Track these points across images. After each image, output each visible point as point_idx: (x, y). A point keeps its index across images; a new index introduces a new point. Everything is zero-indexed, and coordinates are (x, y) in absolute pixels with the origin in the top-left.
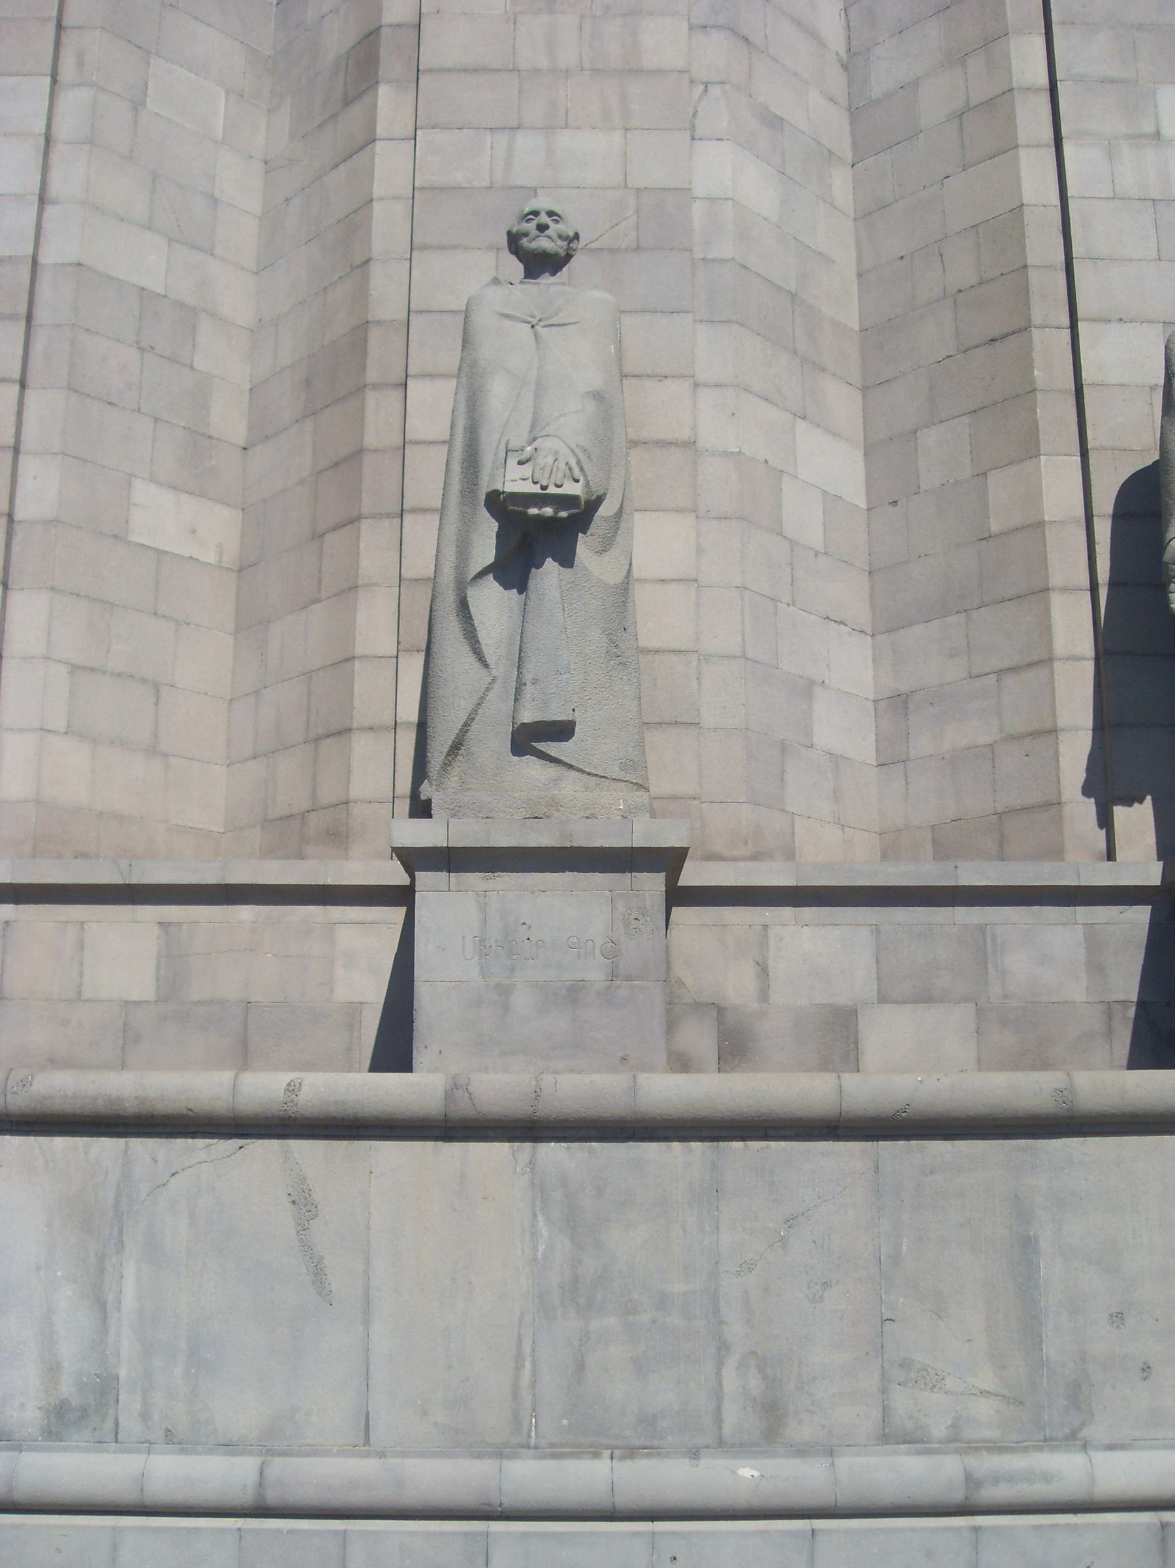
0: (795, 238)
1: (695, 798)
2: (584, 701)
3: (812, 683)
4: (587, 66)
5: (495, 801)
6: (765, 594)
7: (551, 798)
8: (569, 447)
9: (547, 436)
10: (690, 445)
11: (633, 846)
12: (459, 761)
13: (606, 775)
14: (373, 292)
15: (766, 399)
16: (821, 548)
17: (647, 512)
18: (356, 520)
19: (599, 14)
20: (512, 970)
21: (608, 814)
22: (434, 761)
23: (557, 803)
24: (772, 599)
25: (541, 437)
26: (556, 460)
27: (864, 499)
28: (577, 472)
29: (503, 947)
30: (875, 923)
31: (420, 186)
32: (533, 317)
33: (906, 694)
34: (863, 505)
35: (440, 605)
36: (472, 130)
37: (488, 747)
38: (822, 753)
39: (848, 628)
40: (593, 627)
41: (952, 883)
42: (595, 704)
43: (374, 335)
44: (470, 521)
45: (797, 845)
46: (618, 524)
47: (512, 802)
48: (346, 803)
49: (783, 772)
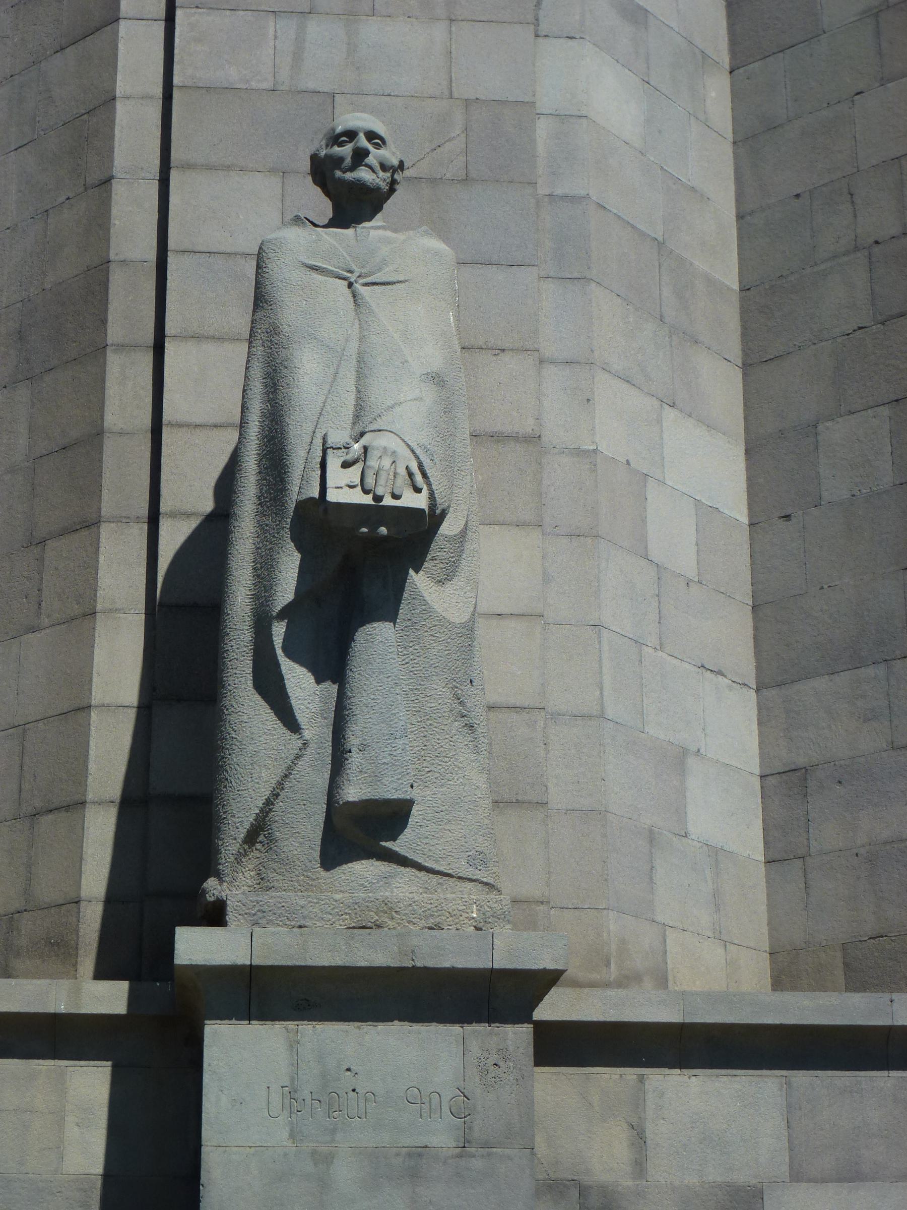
3: (684, 752)
5: (309, 905)
6: (627, 634)
7: (384, 901)
8: (408, 445)
9: (380, 431)
10: (532, 440)
11: (495, 967)
12: (256, 849)
13: (451, 871)
14: (117, 222)
15: (628, 381)
16: (692, 574)
20: (334, 1131)
22: (226, 850)
23: (391, 909)
24: (636, 642)
26: (394, 462)
27: (746, 512)
28: (419, 478)
29: (320, 1101)
31: (181, 85)
32: (351, 272)
33: (805, 768)
34: (744, 519)
36: (250, 13)
37: (298, 833)
39: (727, 681)
40: (434, 678)
41: (888, 1022)
43: (117, 279)
44: (274, 537)
45: (670, 966)
46: (462, 546)
48: (76, 902)
49: (652, 869)
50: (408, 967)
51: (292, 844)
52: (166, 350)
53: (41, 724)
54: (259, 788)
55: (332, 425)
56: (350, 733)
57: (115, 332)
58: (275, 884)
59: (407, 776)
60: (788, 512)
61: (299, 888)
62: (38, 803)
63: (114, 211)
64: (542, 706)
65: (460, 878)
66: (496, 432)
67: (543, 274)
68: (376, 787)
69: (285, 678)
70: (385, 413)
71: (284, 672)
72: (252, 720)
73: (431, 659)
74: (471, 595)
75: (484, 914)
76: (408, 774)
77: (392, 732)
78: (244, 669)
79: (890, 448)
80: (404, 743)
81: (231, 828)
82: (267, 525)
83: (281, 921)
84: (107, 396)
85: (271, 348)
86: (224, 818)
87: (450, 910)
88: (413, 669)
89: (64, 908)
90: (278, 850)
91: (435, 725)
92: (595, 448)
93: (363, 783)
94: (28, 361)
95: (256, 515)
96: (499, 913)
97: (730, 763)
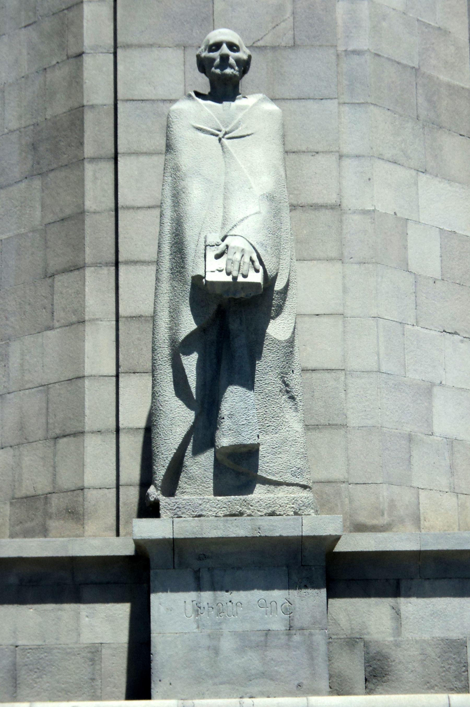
0: (418, 20)
1: (344, 482)
2: (265, 427)
7: (244, 500)
8: (251, 244)
9: (235, 235)
11: (303, 534)
14: (87, 81)
15: (395, 163)
16: (438, 275)
17: (305, 261)
18: (81, 268)
21: (284, 511)
23: (249, 504)
25: (231, 235)
35: (159, 355)
37: (197, 462)
38: (440, 439)
40: (270, 373)
42: (273, 429)
43: (89, 117)
47: (217, 504)
48: (82, 489)
49: (410, 457)
50: (257, 537)
51: (195, 469)
52: (118, 162)
53: (57, 385)
54: (176, 438)
55: (210, 229)
56: (224, 408)
58: (187, 490)
59: (256, 431)
61: (199, 492)
62: (58, 431)
64: (343, 368)
66: (314, 204)
67: (341, 101)
68: (239, 438)
69: (188, 376)
70: (238, 224)
71: (187, 373)
72: (171, 400)
73: (269, 363)
74: (291, 322)
75: (299, 505)
76: (256, 430)
77: (246, 407)
78: (165, 370)
80: (253, 413)
83: (189, 513)
84: (85, 190)
85: (176, 179)
86: (158, 455)
88: (258, 369)
89: (75, 492)
91: (272, 399)
92: (374, 208)
93: (231, 436)
94: (38, 163)
95: (170, 280)
96: (307, 504)
97: (462, 387)
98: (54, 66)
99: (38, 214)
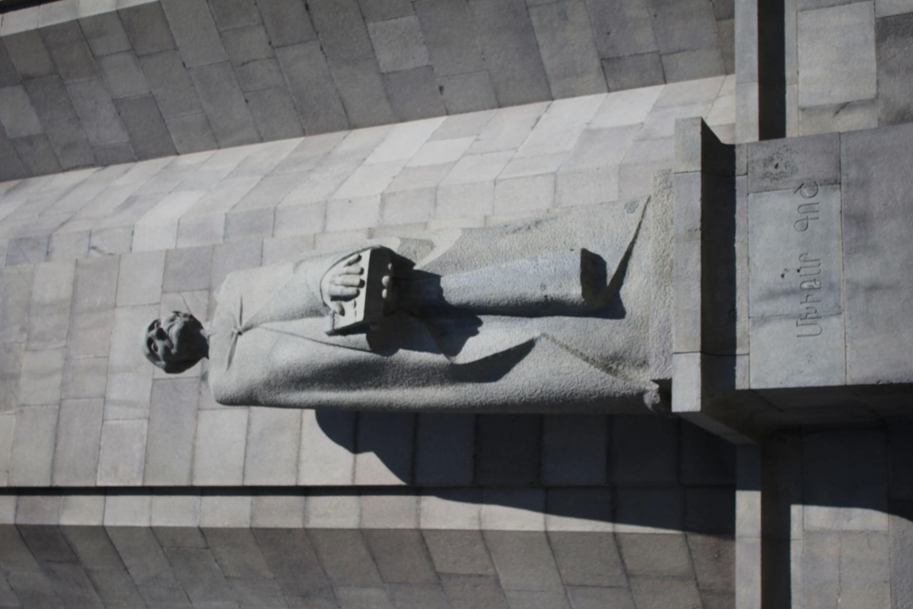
4: (63, 343)
7: (656, 262)
13: (638, 223)
16: (473, 138)
19: (25, 335)
23: (661, 256)
30: (795, 13)
37: (609, 336)
40: (498, 245)
44: (398, 369)
53: (563, 572)
57: (294, 522)
60: (437, 88)
62: (619, 572)
63: (219, 525)
65: (643, 216)
75: (665, 189)
79: (393, 20)
81: (605, 387)
82: (393, 377)
87: (662, 213)
90: (622, 351)
91: (532, 241)
96: (663, 178)
98: (220, 566)
99: (373, 593)
